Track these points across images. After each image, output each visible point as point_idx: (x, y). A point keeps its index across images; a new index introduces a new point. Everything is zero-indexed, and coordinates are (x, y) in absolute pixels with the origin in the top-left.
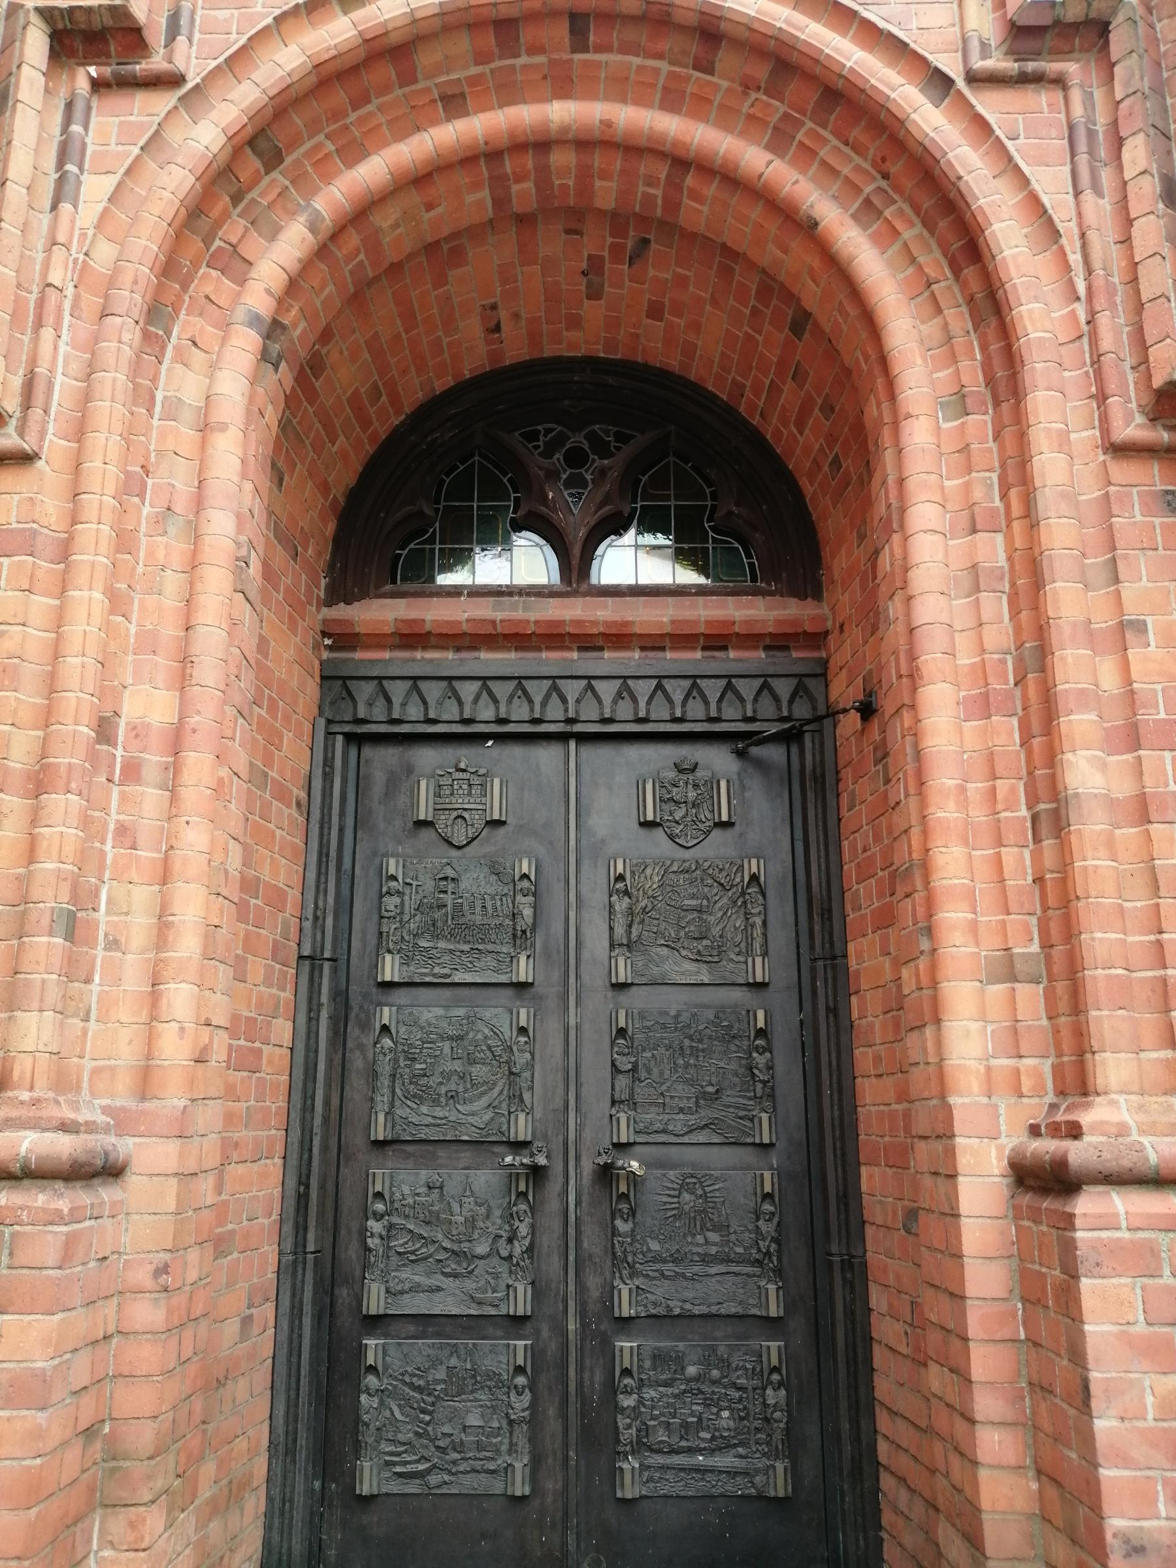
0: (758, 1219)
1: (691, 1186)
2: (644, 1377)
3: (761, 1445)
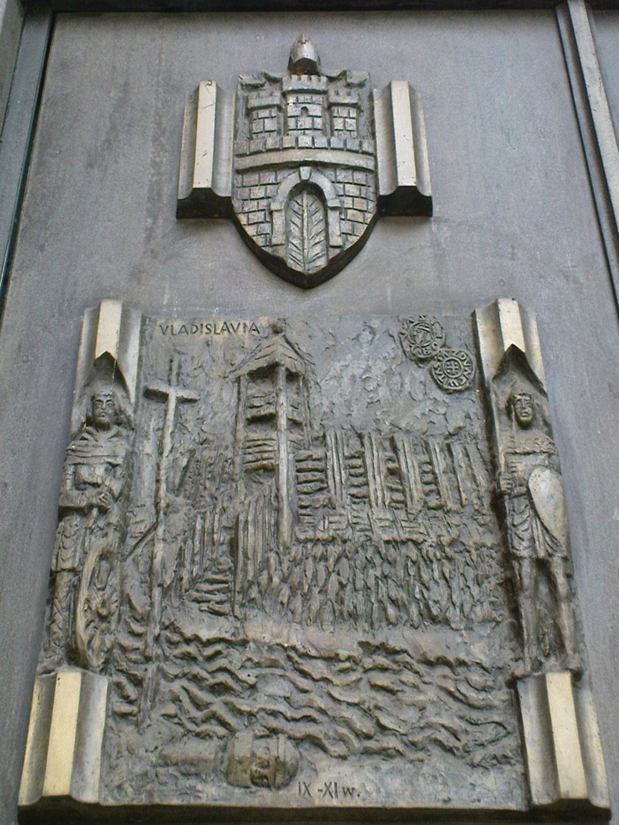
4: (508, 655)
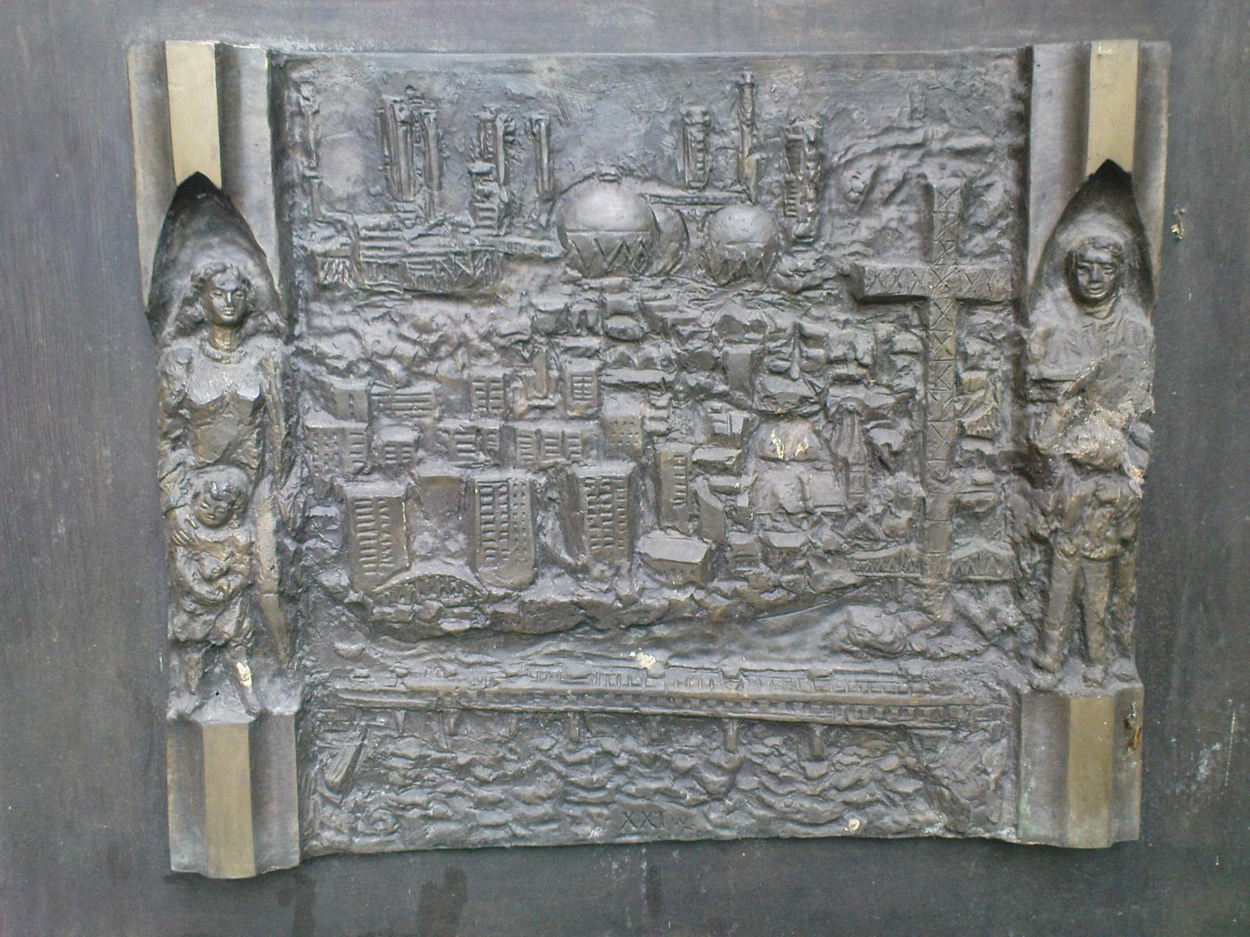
2: (315, 240)
3: (977, 588)
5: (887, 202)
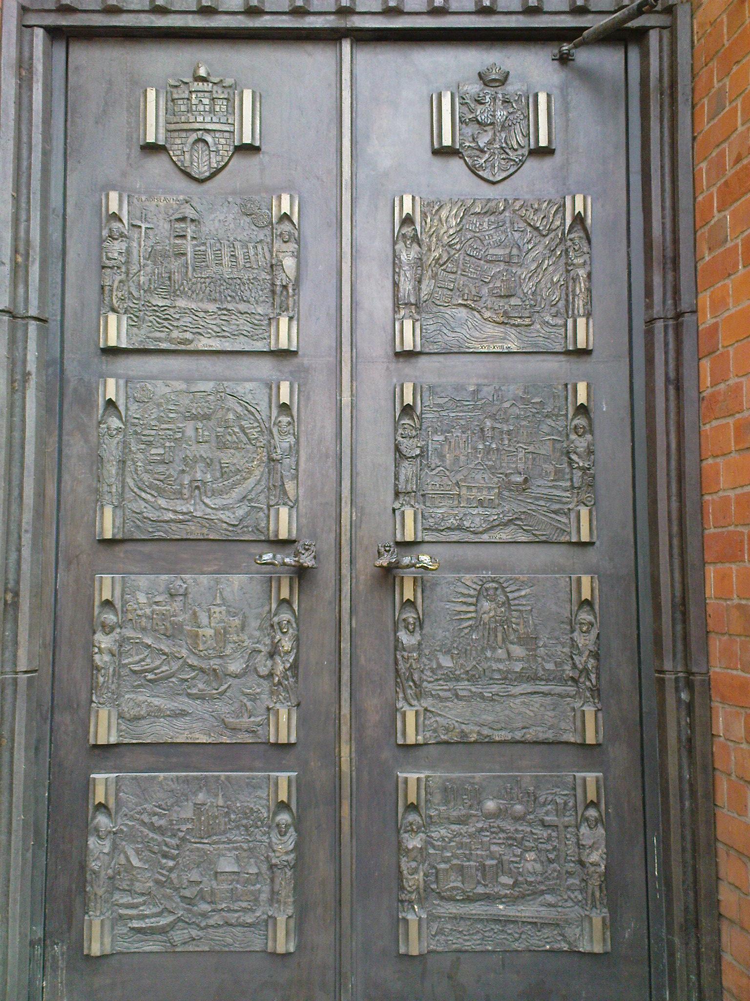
0: (572, 631)
1: (491, 592)
2: (433, 813)
3: (573, 891)
4: (270, 311)
5: (549, 804)
